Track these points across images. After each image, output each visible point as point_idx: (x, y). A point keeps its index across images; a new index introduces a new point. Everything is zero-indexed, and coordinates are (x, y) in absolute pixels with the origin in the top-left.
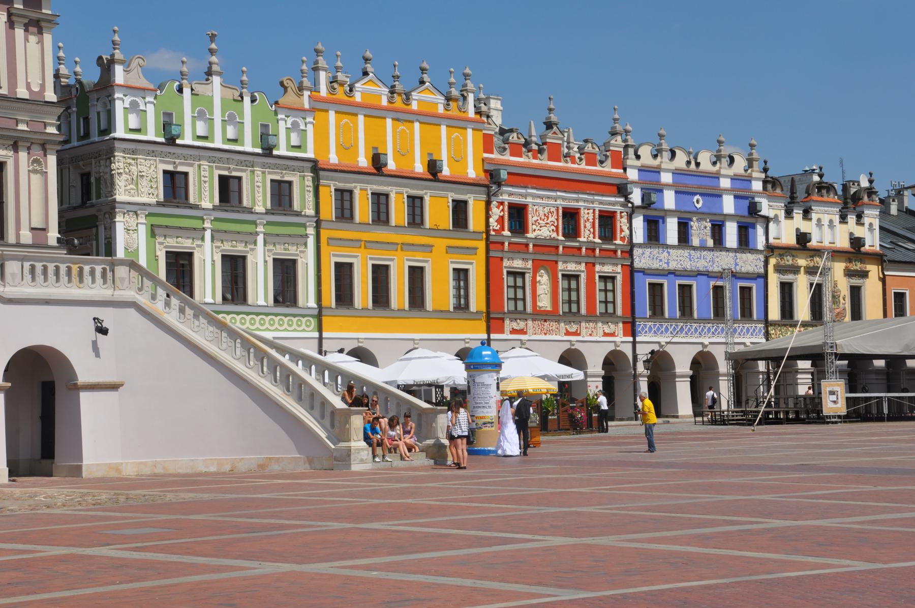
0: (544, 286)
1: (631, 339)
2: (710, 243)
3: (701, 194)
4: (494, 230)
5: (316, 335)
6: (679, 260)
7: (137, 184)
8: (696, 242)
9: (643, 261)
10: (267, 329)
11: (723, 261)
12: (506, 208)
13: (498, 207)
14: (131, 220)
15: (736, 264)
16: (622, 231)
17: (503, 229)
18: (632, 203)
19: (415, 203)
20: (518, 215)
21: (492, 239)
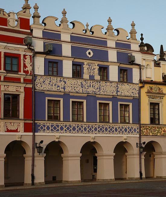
1: (31, 134)
2: (98, 77)
3: (91, 49)
6: (73, 86)
8: (86, 76)
9: (44, 86)
11: (108, 89)
15: (117, 91)
16: (25, 66)
18: (33, 50)
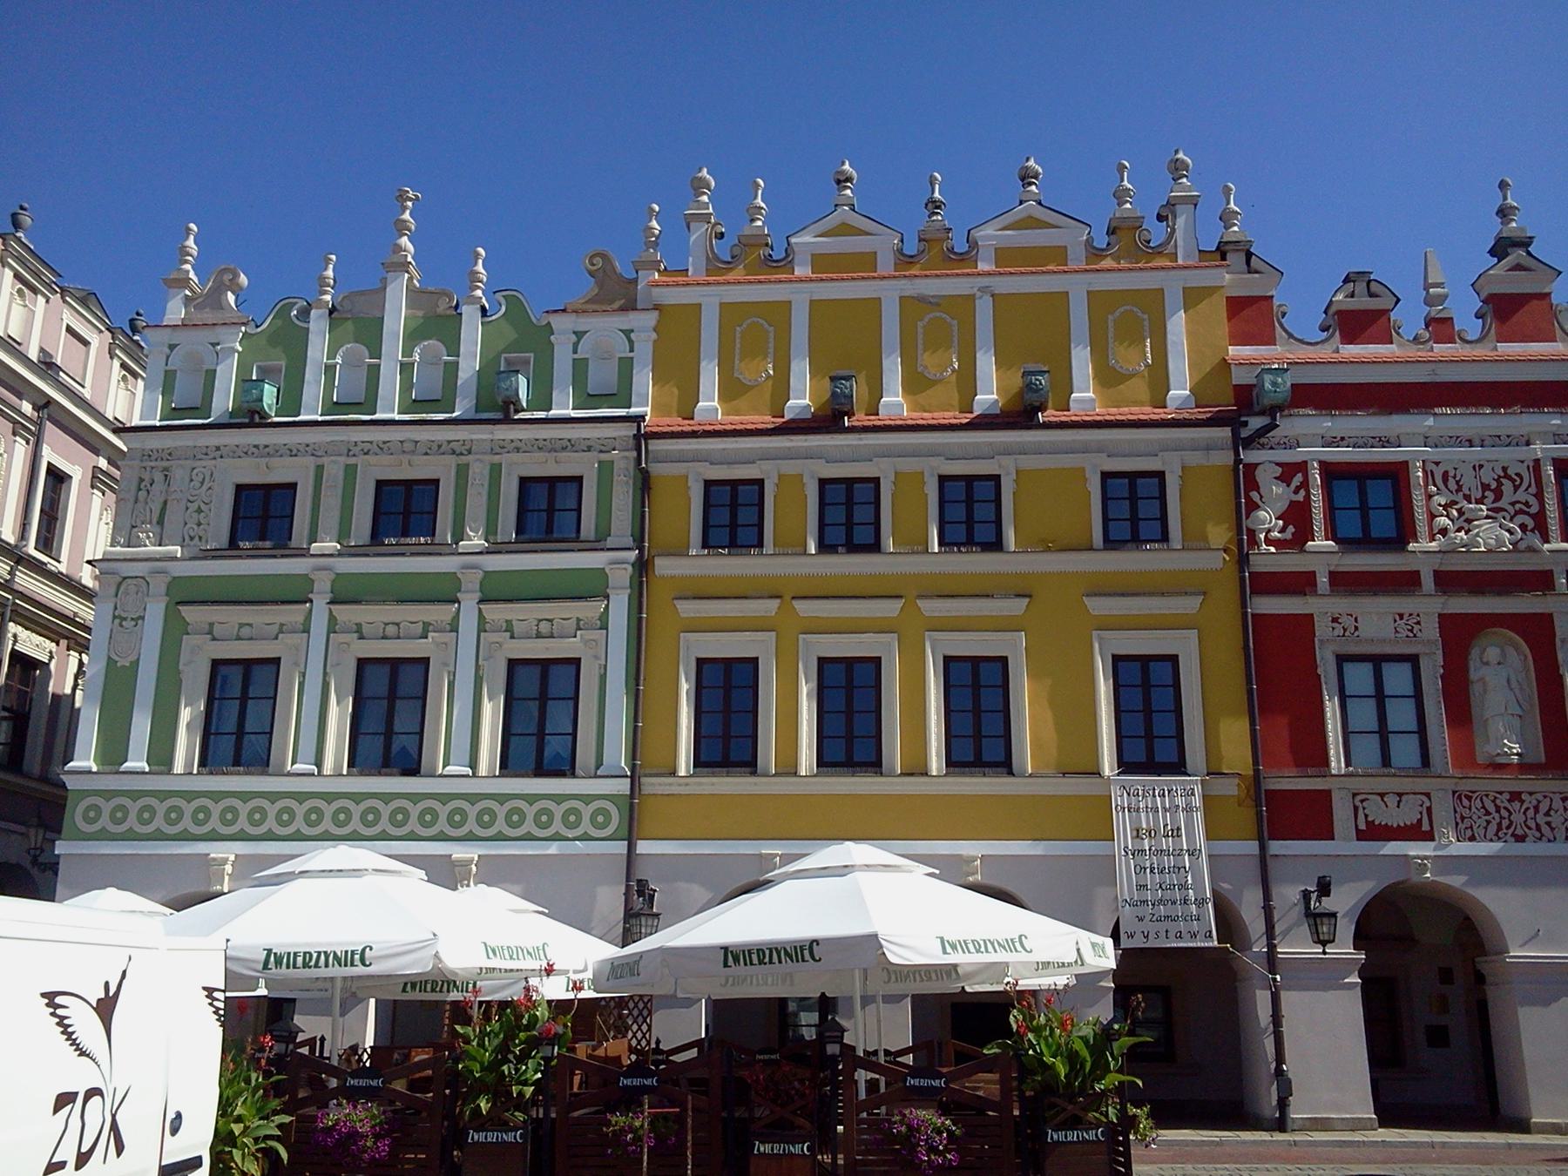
4: (1268, 542)
5: (621, 847)
10: (470, 838)
12: (1316, 477)
17: (1303, 534)
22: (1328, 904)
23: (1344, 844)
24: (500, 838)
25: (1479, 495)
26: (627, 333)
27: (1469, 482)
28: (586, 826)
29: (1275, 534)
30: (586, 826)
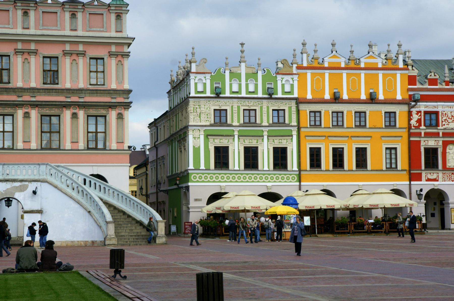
0: (452, 155)
4: (414, 126)
7: (200, 117)
10: (269, 182)
12: (423, 114)
13: (417, 114)
14: (197, 134)
17: (420, 125)
19: (360, 115)
20: (433, 118)
21: (412, 131)
22: (421, 193)
23: (424, 182)
24: (275, 182)
25: (451, 117)
26: (293, 79)
27: (450, 115)
28: (291, 180)
29: (415, 125)
30: (291, 180)
